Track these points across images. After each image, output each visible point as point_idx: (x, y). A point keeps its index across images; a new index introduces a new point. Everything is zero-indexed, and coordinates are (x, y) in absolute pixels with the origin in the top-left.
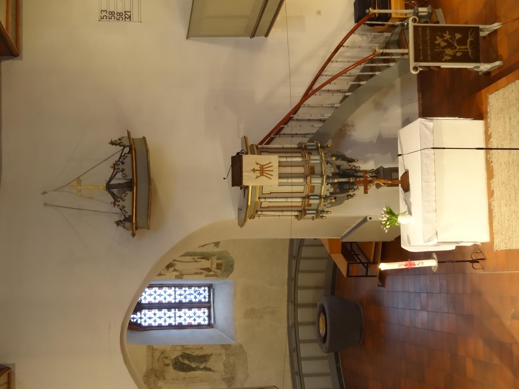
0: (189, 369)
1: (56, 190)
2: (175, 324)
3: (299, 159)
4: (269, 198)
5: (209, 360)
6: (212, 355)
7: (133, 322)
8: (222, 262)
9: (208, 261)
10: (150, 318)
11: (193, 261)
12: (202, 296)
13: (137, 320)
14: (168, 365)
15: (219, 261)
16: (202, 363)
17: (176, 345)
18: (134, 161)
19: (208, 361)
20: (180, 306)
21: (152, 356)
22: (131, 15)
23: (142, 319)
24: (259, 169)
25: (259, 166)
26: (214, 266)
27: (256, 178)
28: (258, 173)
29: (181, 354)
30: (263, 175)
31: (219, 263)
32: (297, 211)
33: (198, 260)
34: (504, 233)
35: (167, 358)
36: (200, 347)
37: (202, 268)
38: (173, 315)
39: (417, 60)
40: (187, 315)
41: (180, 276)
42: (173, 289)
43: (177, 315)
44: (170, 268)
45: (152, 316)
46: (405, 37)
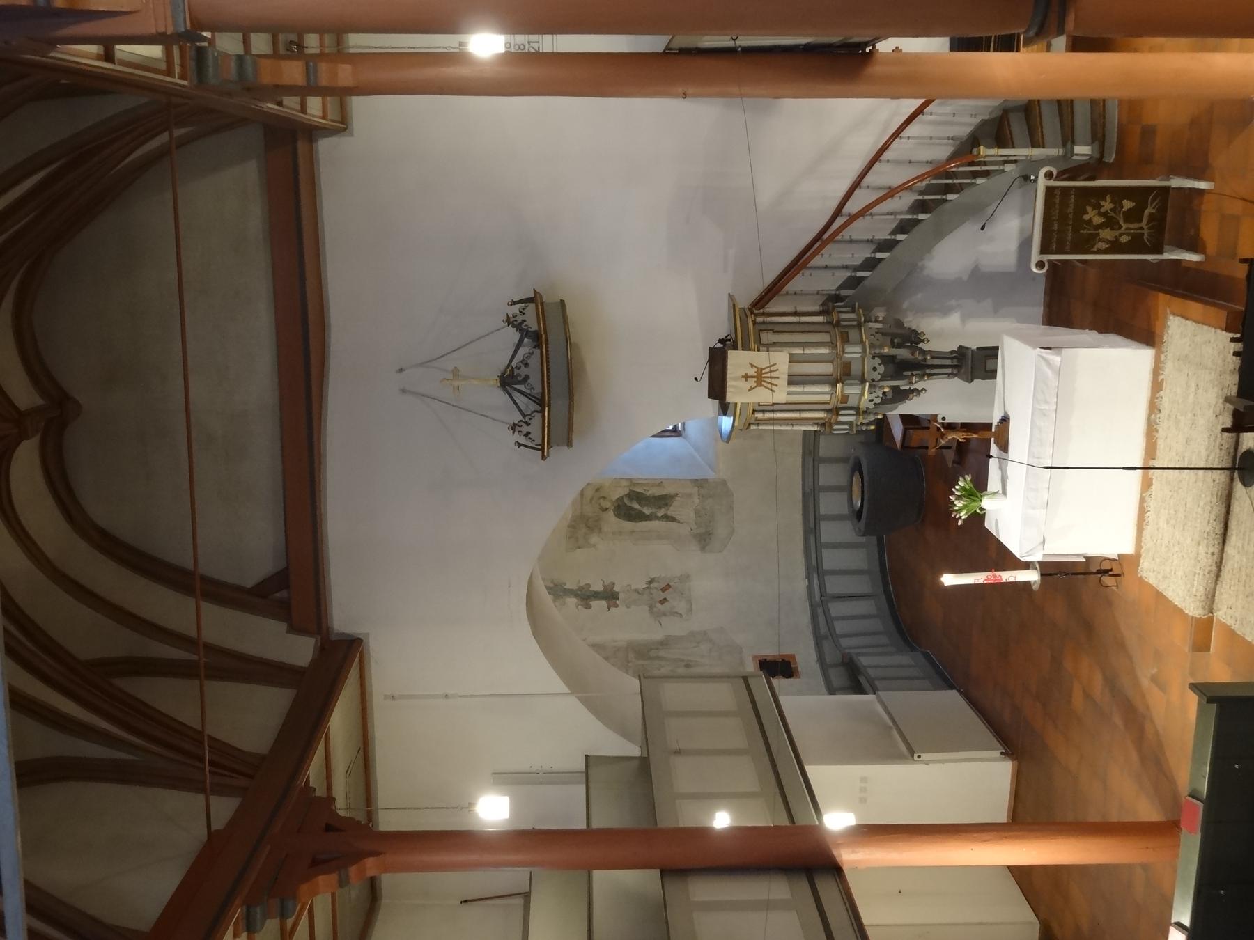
0: (640, 517)
1: (422, 365)
3: (825, 351)
4: (770, 411)
18: (545, 361)
22: (539, 48)
24: (755, 374)
25: (755, 370)
27: (749, 390)
28: (752, 382)
29: (626, 493)
30: (761, 385)
32: (818, 424)
34: (1158, 560)
36: (658, 482)
39: (1044, 250)
46: (1040, 109)
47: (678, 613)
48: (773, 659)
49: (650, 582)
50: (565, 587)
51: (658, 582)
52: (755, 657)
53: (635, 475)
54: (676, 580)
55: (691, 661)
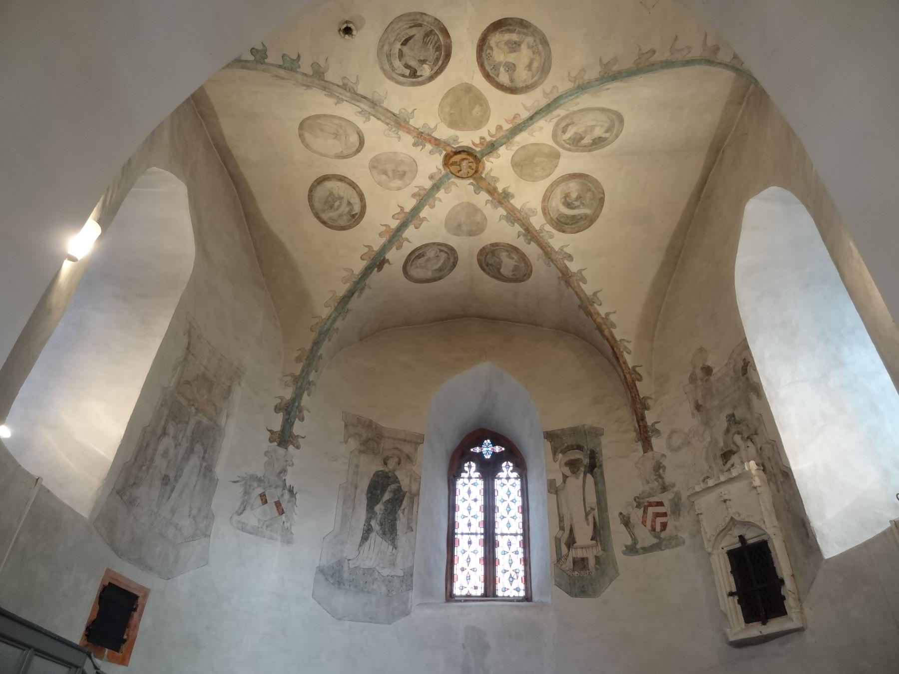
0: (373, 500)
2: (457, 534)
5: (385, 540)
6: (395, 547)
7: (464, 467)
8: (591, 570)
9: (590, 538)
10: (469, 492)
11: (588, 509)
12: (507, 585)
13: (466, 472)
14: (385, 464)
15: (592, 563)
16: (381, 524)
17: (420, 482)
19: (382, 538)
20: (490, 541)
21: (405, 441)
23: (468, 480)
26: (580, 554)
29: (402, 488)
31: (588, 563)
35: (399, 463)
38: (473, 530)
40: (472, 556)
41: (553, 488)
42: (521, 531)
43: (473, 537)
44: (570, 469)
45: (473, 496)
47: (244, 510)
48: (133, 622)
49: (291, 491)
50: (305, 395)
51: (289, 501)
52: (146, 593)
53: (423, 501)
54: (285, 524)
55: (173, 490)
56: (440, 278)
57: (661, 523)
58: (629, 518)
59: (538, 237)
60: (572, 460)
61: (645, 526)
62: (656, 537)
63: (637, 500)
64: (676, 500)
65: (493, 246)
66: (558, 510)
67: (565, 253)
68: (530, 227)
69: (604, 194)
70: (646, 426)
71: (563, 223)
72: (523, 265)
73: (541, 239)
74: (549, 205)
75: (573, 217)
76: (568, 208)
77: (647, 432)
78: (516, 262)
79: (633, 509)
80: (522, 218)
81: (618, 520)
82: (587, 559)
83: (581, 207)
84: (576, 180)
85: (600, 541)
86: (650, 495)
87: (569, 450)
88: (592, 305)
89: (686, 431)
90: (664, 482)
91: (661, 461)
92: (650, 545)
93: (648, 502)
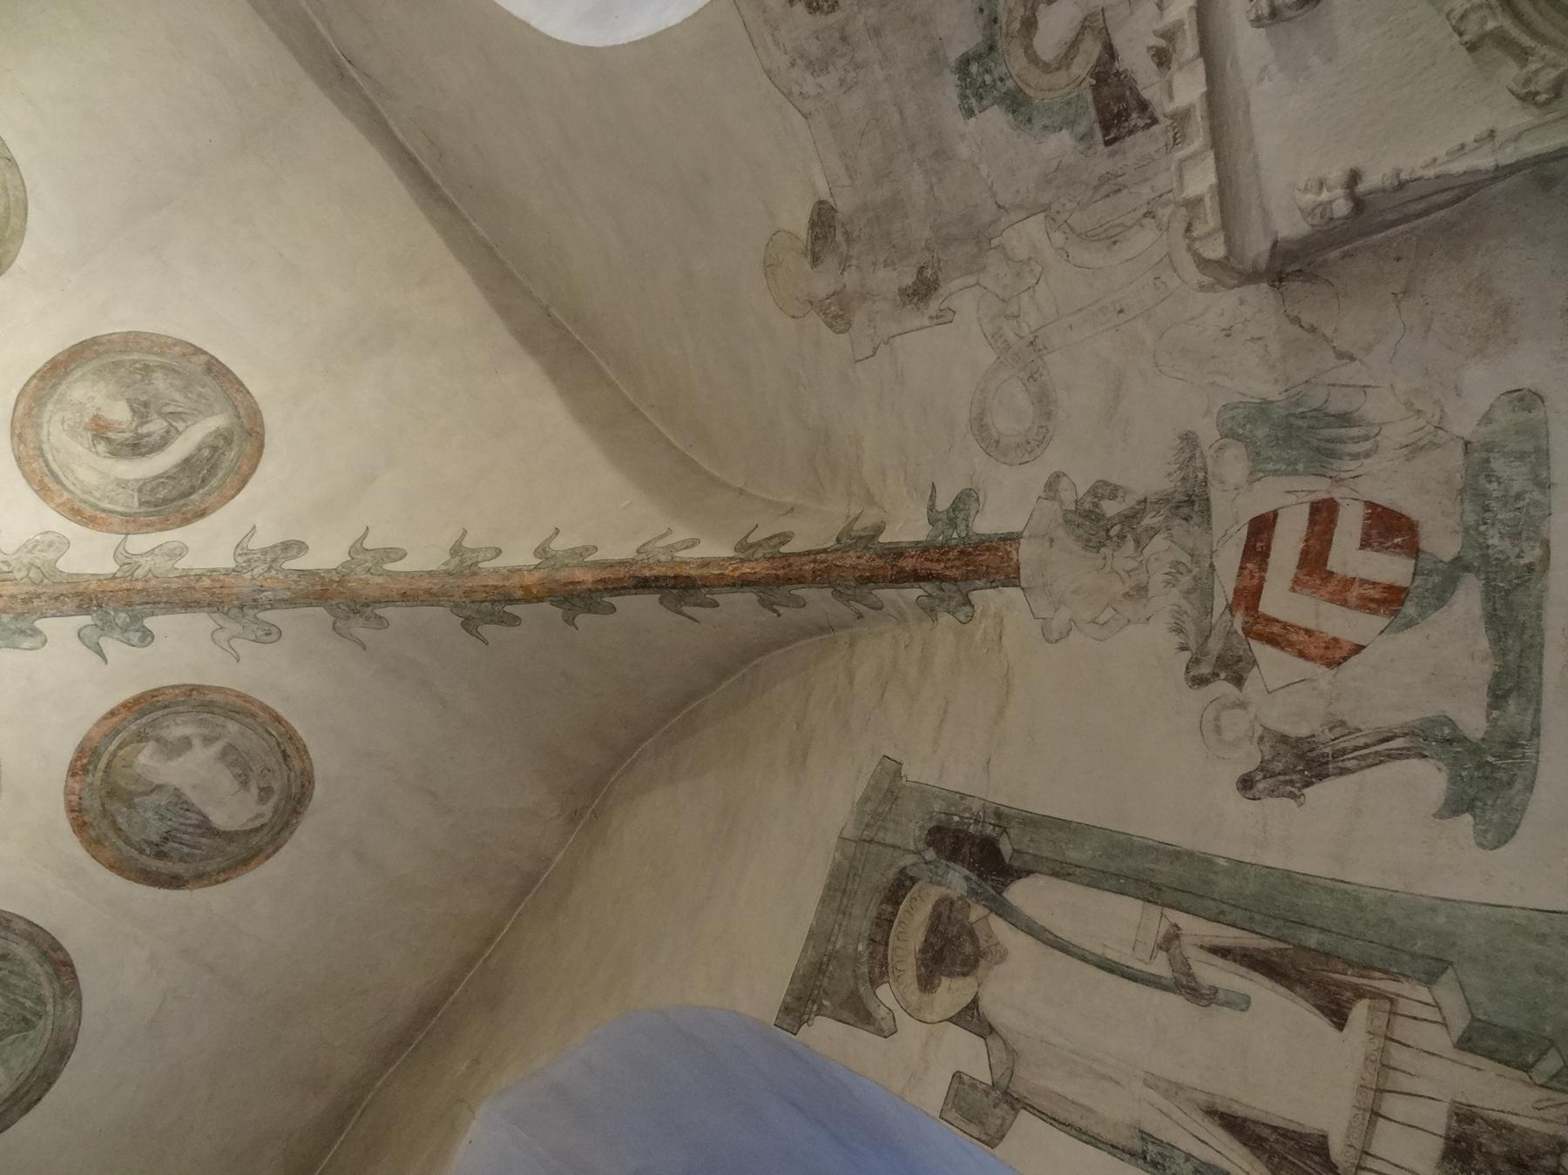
9: (1322, 1024)
11: (1160, 967)
31: (1501, 1129)
33: (1213, 973)
37: (1240, 1111)
44: (951, 975)
56: (61, 1053)
57: (1365, 544)
58: (1284, 739)
59: (139, 585)
60: (927, 946)
61: (1359, 648)
62: (1441, 596)
63: (1205, 669)
64: (1262, 432)
65: (85, 770)
66: (1094, 1141)
67: (264, 551)
68: (81, 588)
69: (199, 351)
70: (924, 549)
71: (174, 500)
72: (233, 727)
73: (153, 582)
74: (78, 492)
75: (187, 464)
76: (143, 455)
77: (944, 549)
78: (208, 741)
79: (1242, 705)
80: (32, 589)
81: (1276, 808)
82: (1464, 1115)
83: (180, 425)
84: (77, 374)
85: (1366, 968)
86: (1203, 590)
87: (887, 944)
88: (474, 574)
89: (988, 357)
90: (1164, 500)
91: (1068, 497)
92: (1484, 644)
93: (1230, 608)
